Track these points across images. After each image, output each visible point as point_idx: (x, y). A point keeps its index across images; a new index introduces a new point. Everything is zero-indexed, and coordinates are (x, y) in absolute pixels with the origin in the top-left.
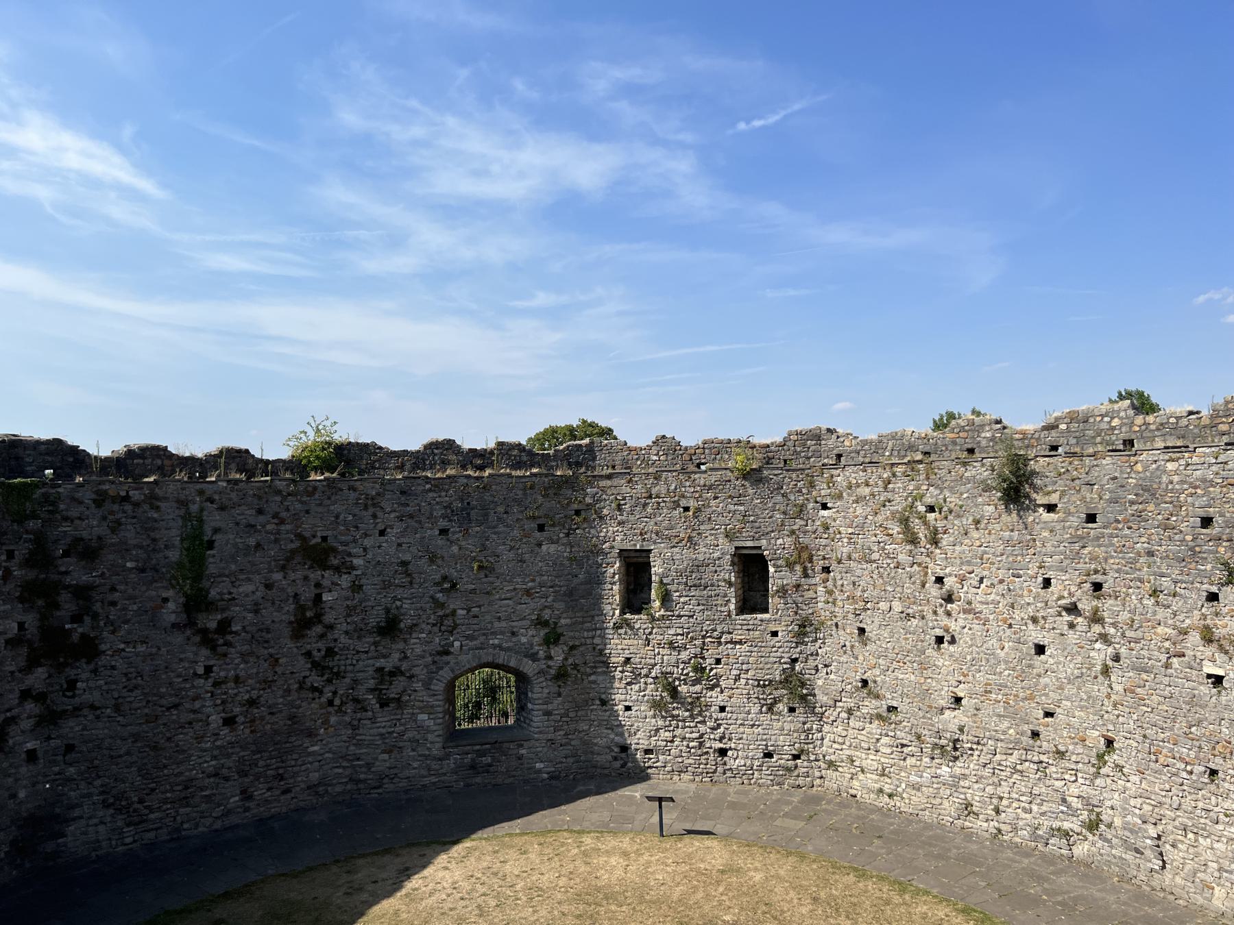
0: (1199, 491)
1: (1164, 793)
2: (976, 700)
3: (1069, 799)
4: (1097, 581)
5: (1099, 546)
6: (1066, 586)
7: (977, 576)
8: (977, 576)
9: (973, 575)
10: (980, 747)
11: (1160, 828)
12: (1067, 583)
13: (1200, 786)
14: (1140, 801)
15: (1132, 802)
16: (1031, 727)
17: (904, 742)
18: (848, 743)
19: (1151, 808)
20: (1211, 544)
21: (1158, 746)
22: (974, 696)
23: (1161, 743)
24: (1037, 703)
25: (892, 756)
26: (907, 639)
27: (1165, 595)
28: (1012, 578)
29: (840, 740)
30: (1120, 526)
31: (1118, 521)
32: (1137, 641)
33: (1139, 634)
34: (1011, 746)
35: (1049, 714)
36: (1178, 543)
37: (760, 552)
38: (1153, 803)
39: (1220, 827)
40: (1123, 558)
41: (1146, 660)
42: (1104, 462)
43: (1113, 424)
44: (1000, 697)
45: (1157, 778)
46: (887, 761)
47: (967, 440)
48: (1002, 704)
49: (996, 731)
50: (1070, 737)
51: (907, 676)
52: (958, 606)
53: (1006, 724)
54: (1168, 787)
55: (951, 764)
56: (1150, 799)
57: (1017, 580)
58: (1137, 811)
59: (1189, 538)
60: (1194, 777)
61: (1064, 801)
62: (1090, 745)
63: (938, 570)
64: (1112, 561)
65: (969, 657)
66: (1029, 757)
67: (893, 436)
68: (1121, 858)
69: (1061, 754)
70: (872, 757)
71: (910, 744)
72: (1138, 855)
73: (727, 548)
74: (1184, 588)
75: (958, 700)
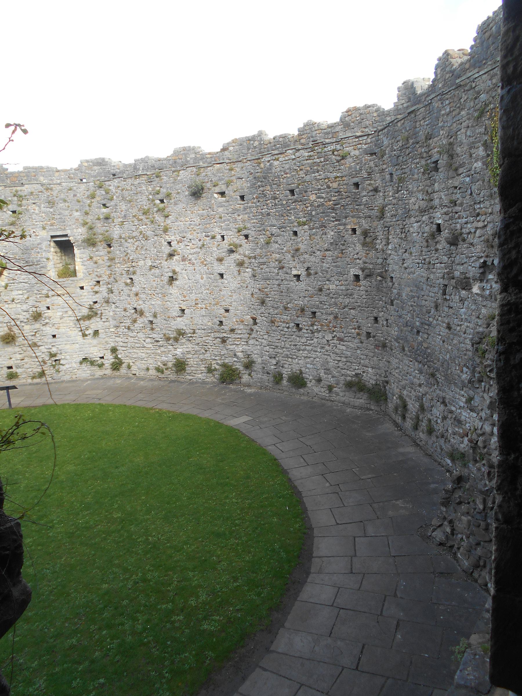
0: (288, 175)
1: (277, 341)
2: (192, 310)
3: (238, 354)
4: (246, 234)
5: (246, 214)
6: (232, 237)
7: (187, 239)
8: (187, 239)
9: (185, 239)
10: (195, 335)
11: (277, 359)
12: (232, 237)
13: (293, 333)
14: (268, 347)
15: (265, 349)
16: (218, 319)
17: (157, 339)
18: (129, 346)
19: (273, 350)
20: (294, 204)
21: (275, 317)
22: (190, 308)
23: (276, 316)
24: (221, 306)
25: (152, 349)
26: (154, 281)
27: (275, 236)
28: (205, 238)
29: (125, 345)
30: (255, 201)
31: (254, 198)
32: (264, 263)
33: (264, 260)
34: (210, 332)
35: (227, 311)
36: (280, 206)
37: (67, 239)
38: (273, 347)
39: (301, 352)
40: (256, 219)
41: (268, 274)
42: (247, 164)
43: (255, 145)
44: (203, 306)
45: (275, 334)
46: (149, 351)
47: (183, 160)
48: (204, 309)
49: (202, 325)
50: (237, 321)
51: (156, 302)
52: (179, 257)
53: (207, 320)
54: (279, 337)
55: (182, 346)
56: (272, 345)
57: (207, 238)
58: (267, 353)
59: (284, 202)
60: (290, 330)
61: (235, 355)
62: (246, 324)
63: (168, 238)
64: (252, 221)
65: (186, 286)
66: (218, 336)
67: (143, 160)
68: (261, 378)
69: (232, 330)
70: (142, 351)
71: (160, 340)
72: (268, 375)
73: (45, 235)
74: (283, 231)
75: (183, 311)
